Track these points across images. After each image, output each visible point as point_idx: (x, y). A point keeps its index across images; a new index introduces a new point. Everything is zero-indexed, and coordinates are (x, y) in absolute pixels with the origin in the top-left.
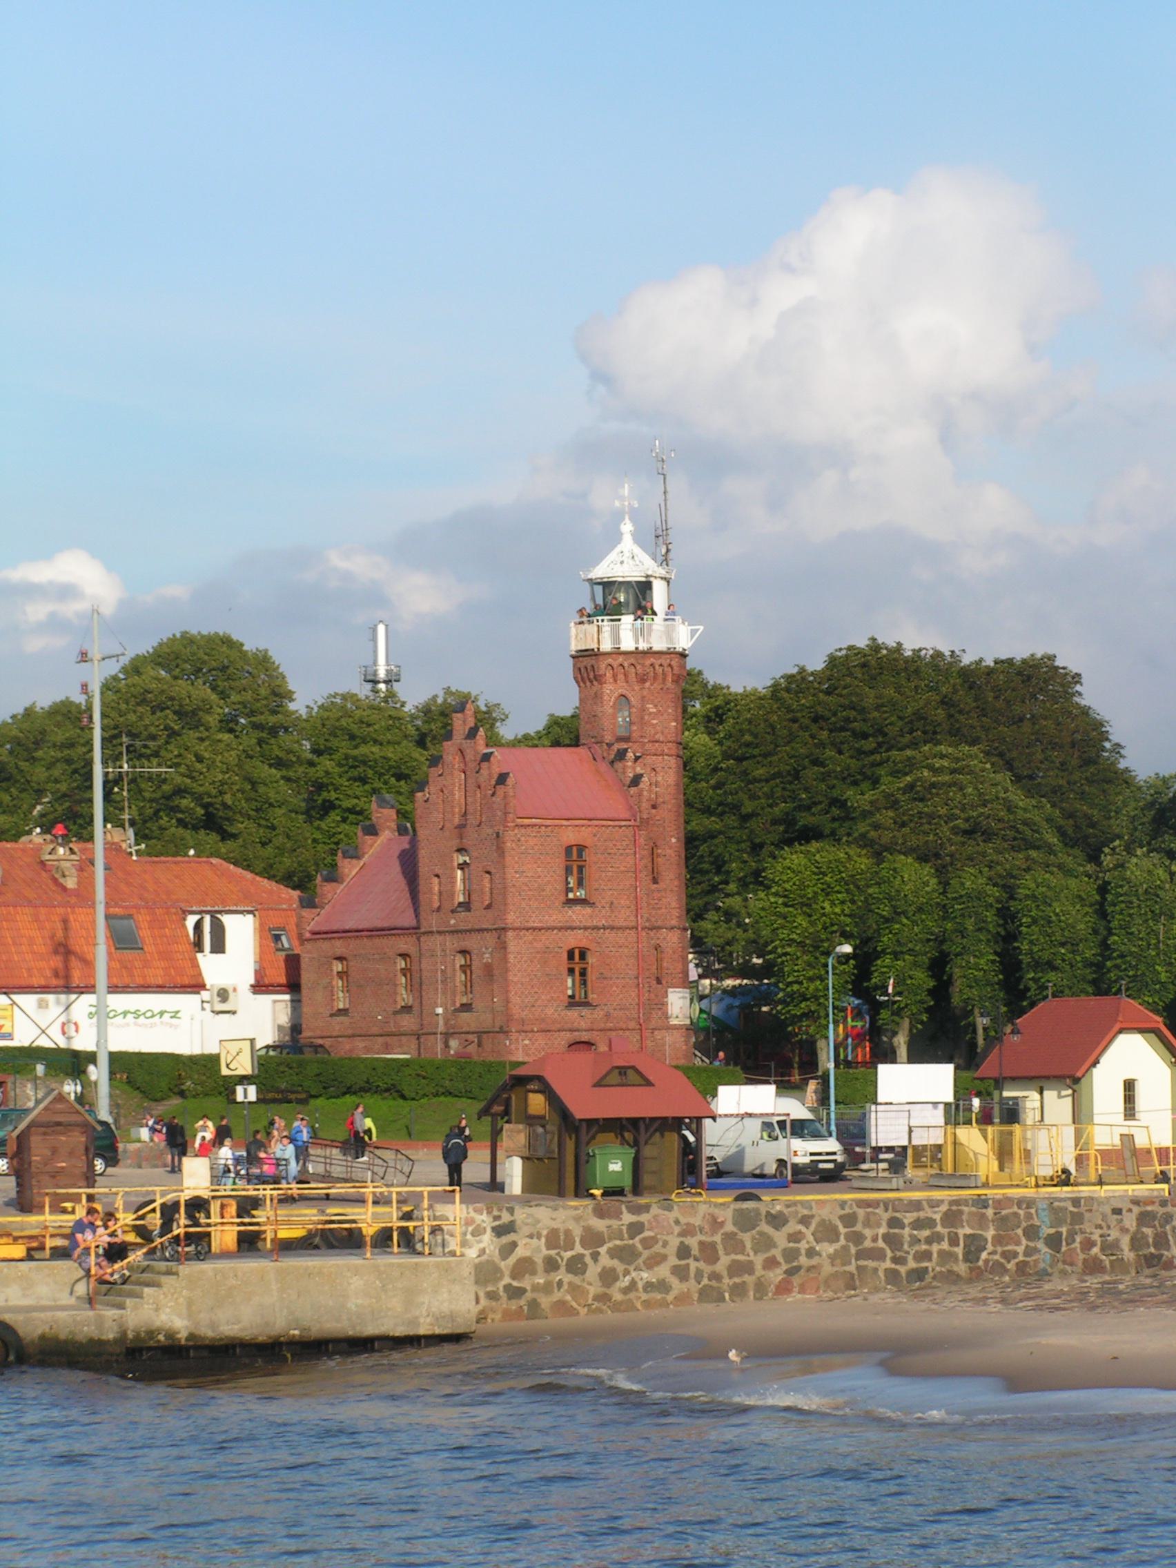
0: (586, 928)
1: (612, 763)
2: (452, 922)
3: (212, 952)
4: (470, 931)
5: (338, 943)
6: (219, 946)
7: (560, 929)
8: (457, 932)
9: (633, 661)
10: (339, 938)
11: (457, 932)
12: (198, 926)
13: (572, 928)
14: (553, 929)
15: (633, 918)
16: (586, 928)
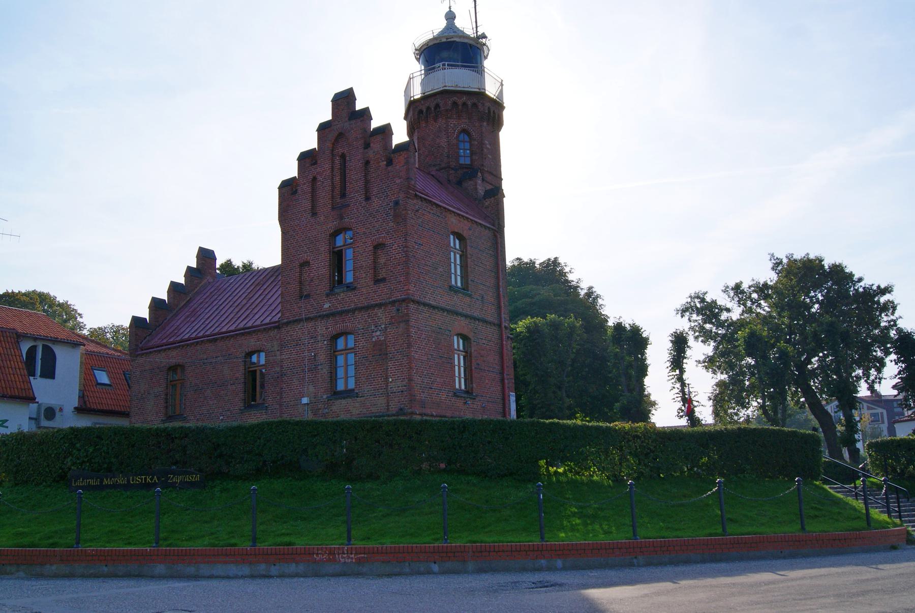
0: (466, 316)
1: (460, 183)
2: (326, 306)
3: (41, 376)
4: (353, 311)
5: (174, 353)
6: (49, 372)
7: (448, 311)
8: (333, 315)
9: (475, 101)
10: (174, 348)
11: (333, 315)
12: (32, 351)
13: (457, 314)
14: (443, 310)
15: (496, 316)
16: (466, 316)
